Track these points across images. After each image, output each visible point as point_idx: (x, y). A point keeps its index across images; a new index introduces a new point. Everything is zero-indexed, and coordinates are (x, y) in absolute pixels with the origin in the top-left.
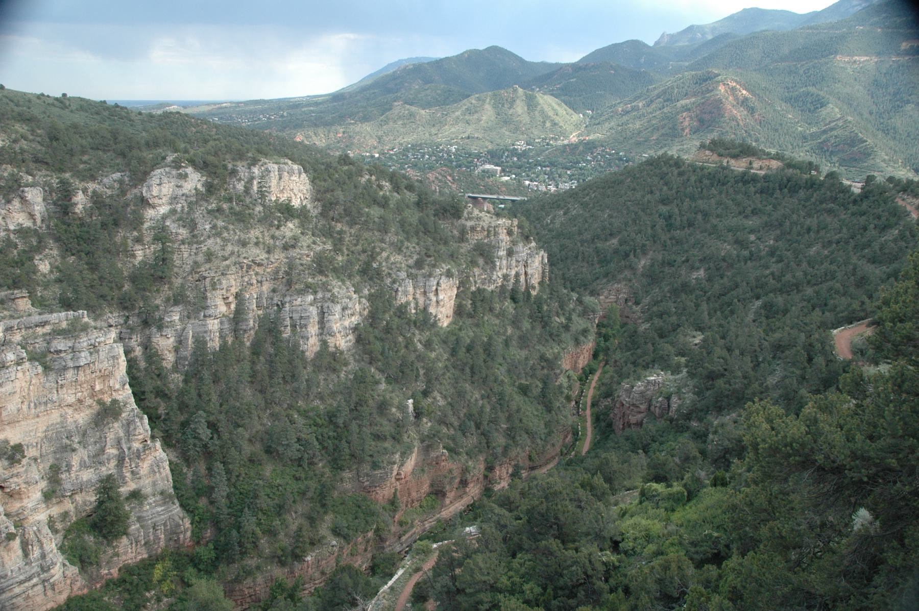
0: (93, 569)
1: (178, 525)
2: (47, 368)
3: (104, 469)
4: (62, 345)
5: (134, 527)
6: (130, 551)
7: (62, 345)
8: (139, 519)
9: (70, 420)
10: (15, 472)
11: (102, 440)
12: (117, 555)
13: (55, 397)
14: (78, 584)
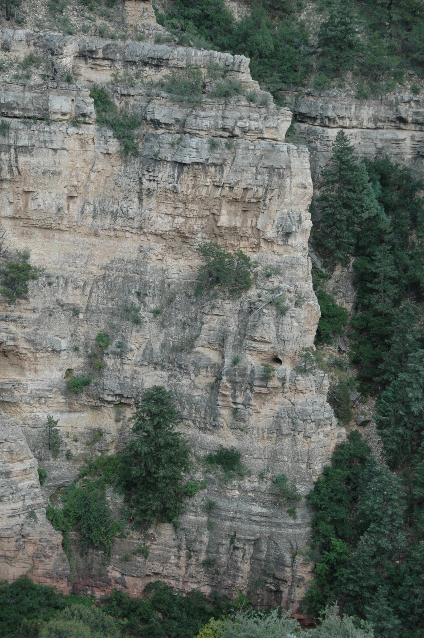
0: (96, 556)
1: (280, 562)
2: (128, 151)
3: (185, 381)
4: (165, 111)
5: (193, 517)
6: (173, 560)
7: (165, 111)
8: (210, 508)
9: (153, 263)
10: (17, 314)
11: (193, 323)
12: (144, 552)
13: (133, 209)
14: (49, 565)
